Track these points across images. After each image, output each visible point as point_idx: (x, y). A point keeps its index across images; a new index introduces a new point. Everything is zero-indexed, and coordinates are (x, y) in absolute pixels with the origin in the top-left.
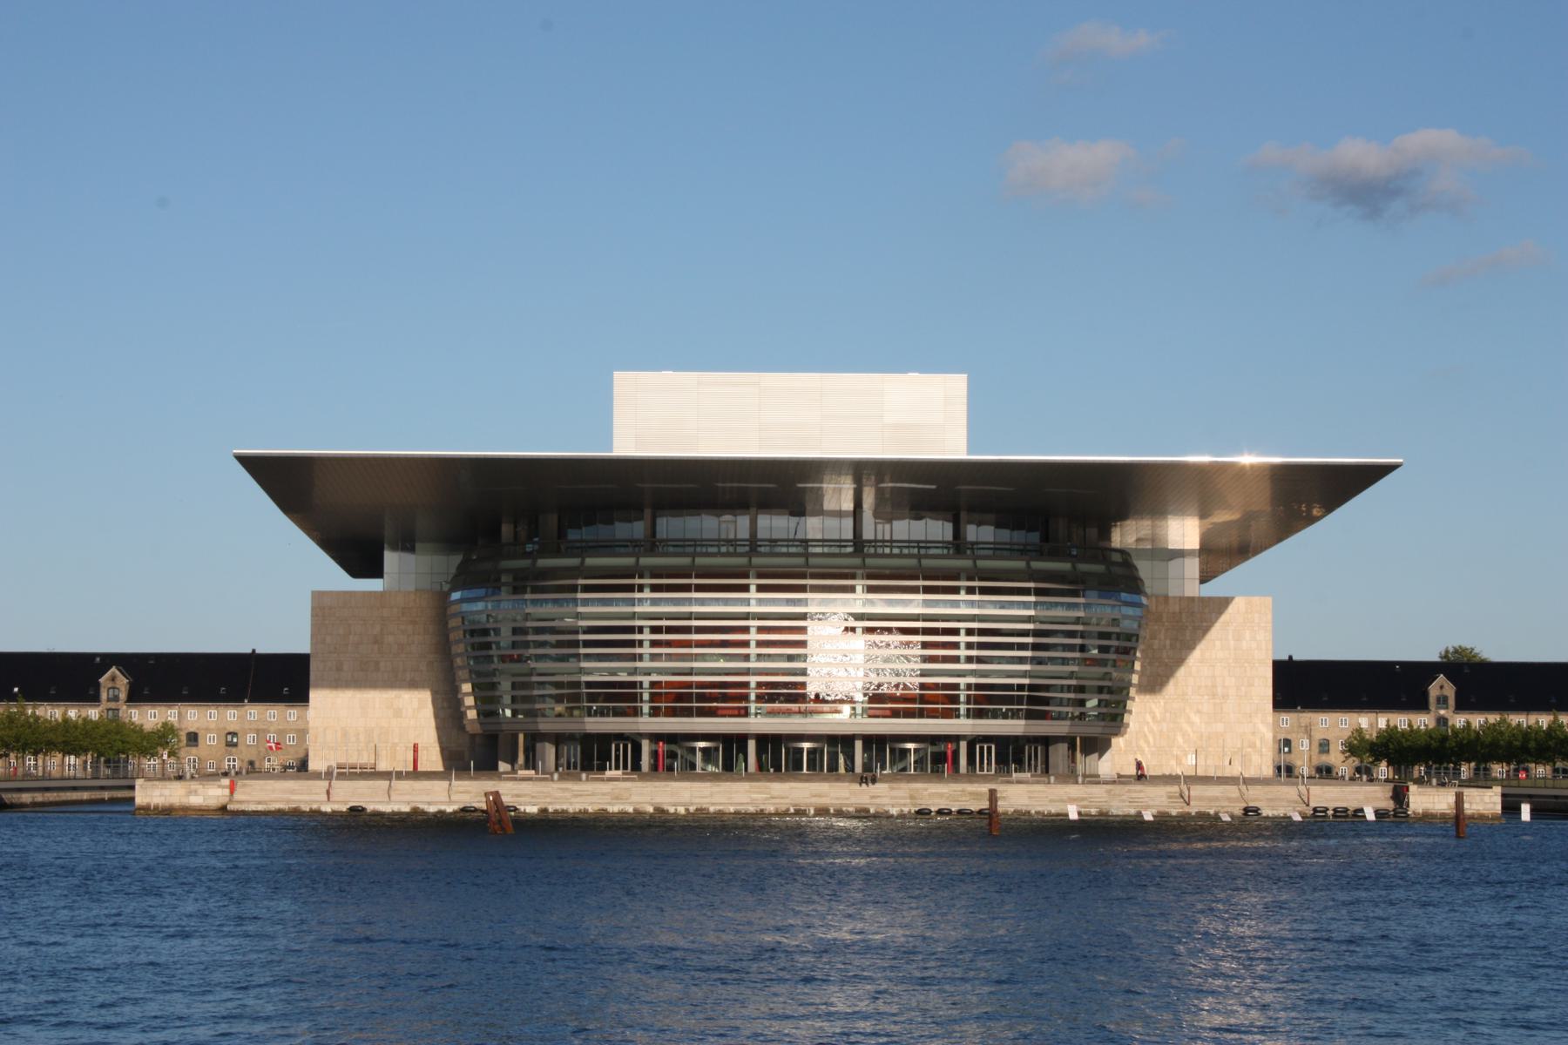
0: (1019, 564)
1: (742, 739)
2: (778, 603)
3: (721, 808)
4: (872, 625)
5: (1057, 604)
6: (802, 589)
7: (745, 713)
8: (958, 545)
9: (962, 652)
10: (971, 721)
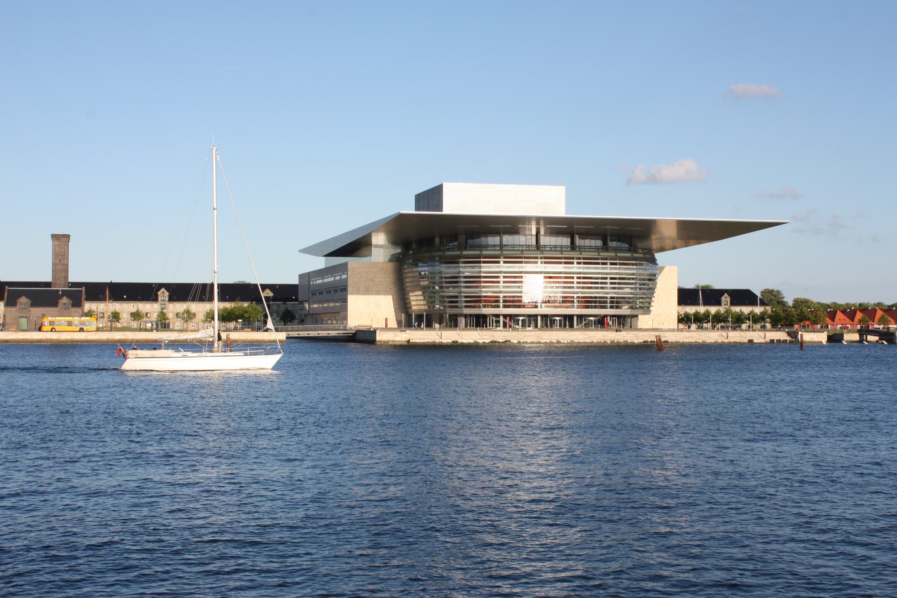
0: (629, 255)
1: (536, 316)
2: (516, 268)
3: (578, 341)
4: (549, 277)
5: (468, 267)
6: (521, 262)
8: (573, 247)
9: (575, 285)
10: (579, 309)
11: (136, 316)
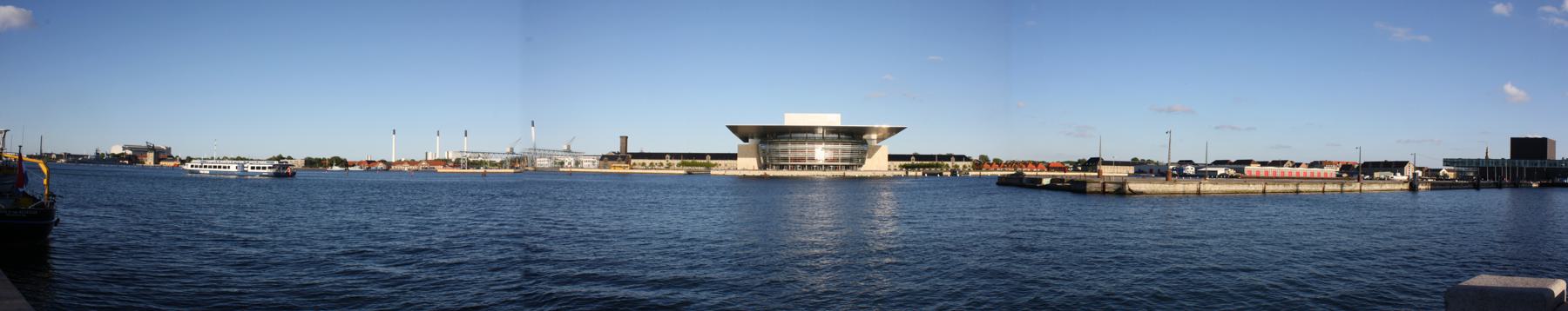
2: (811, 146)
4: (825, 149)
8: (839, 138)
11: (651, 164)
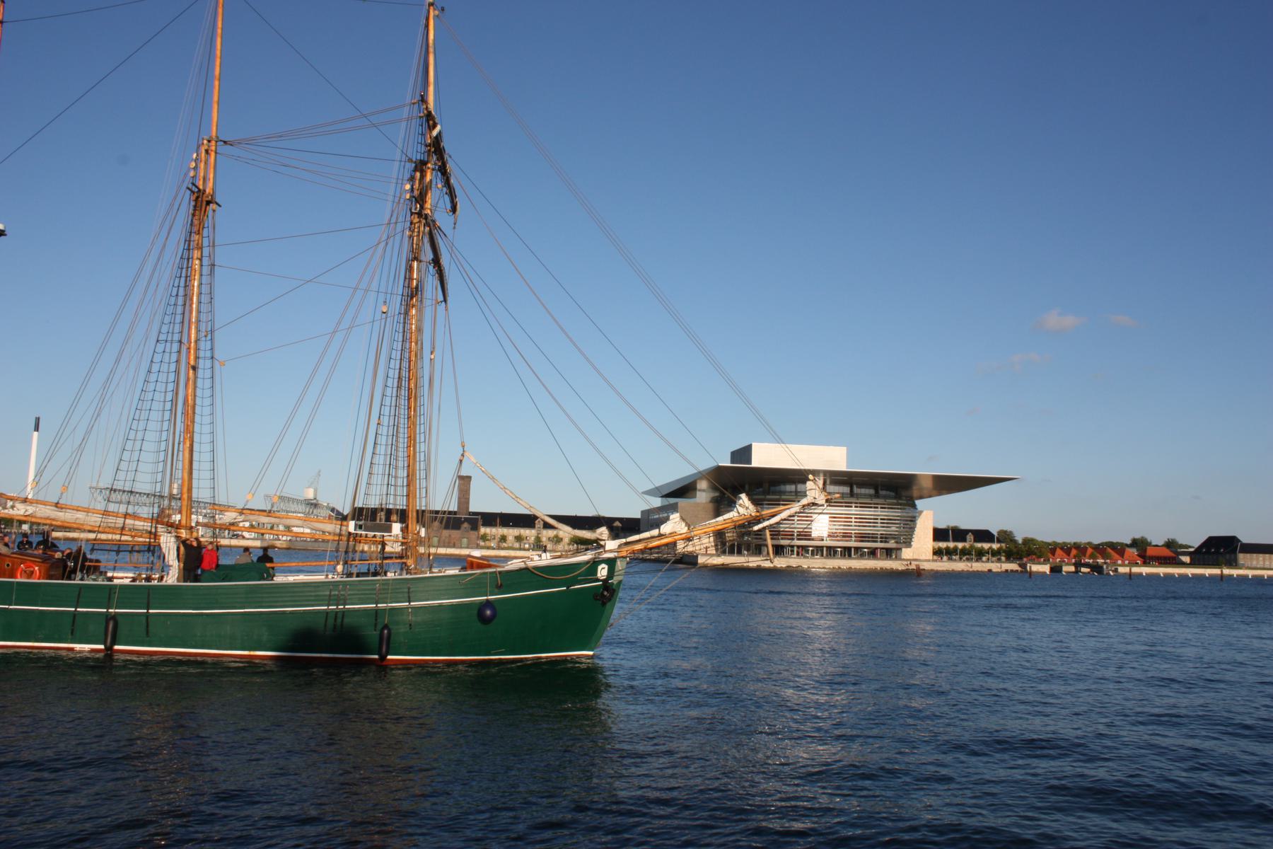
0: (895, 501)
1: (823, 547)
7: (850, 541)
8: (852, 494)
